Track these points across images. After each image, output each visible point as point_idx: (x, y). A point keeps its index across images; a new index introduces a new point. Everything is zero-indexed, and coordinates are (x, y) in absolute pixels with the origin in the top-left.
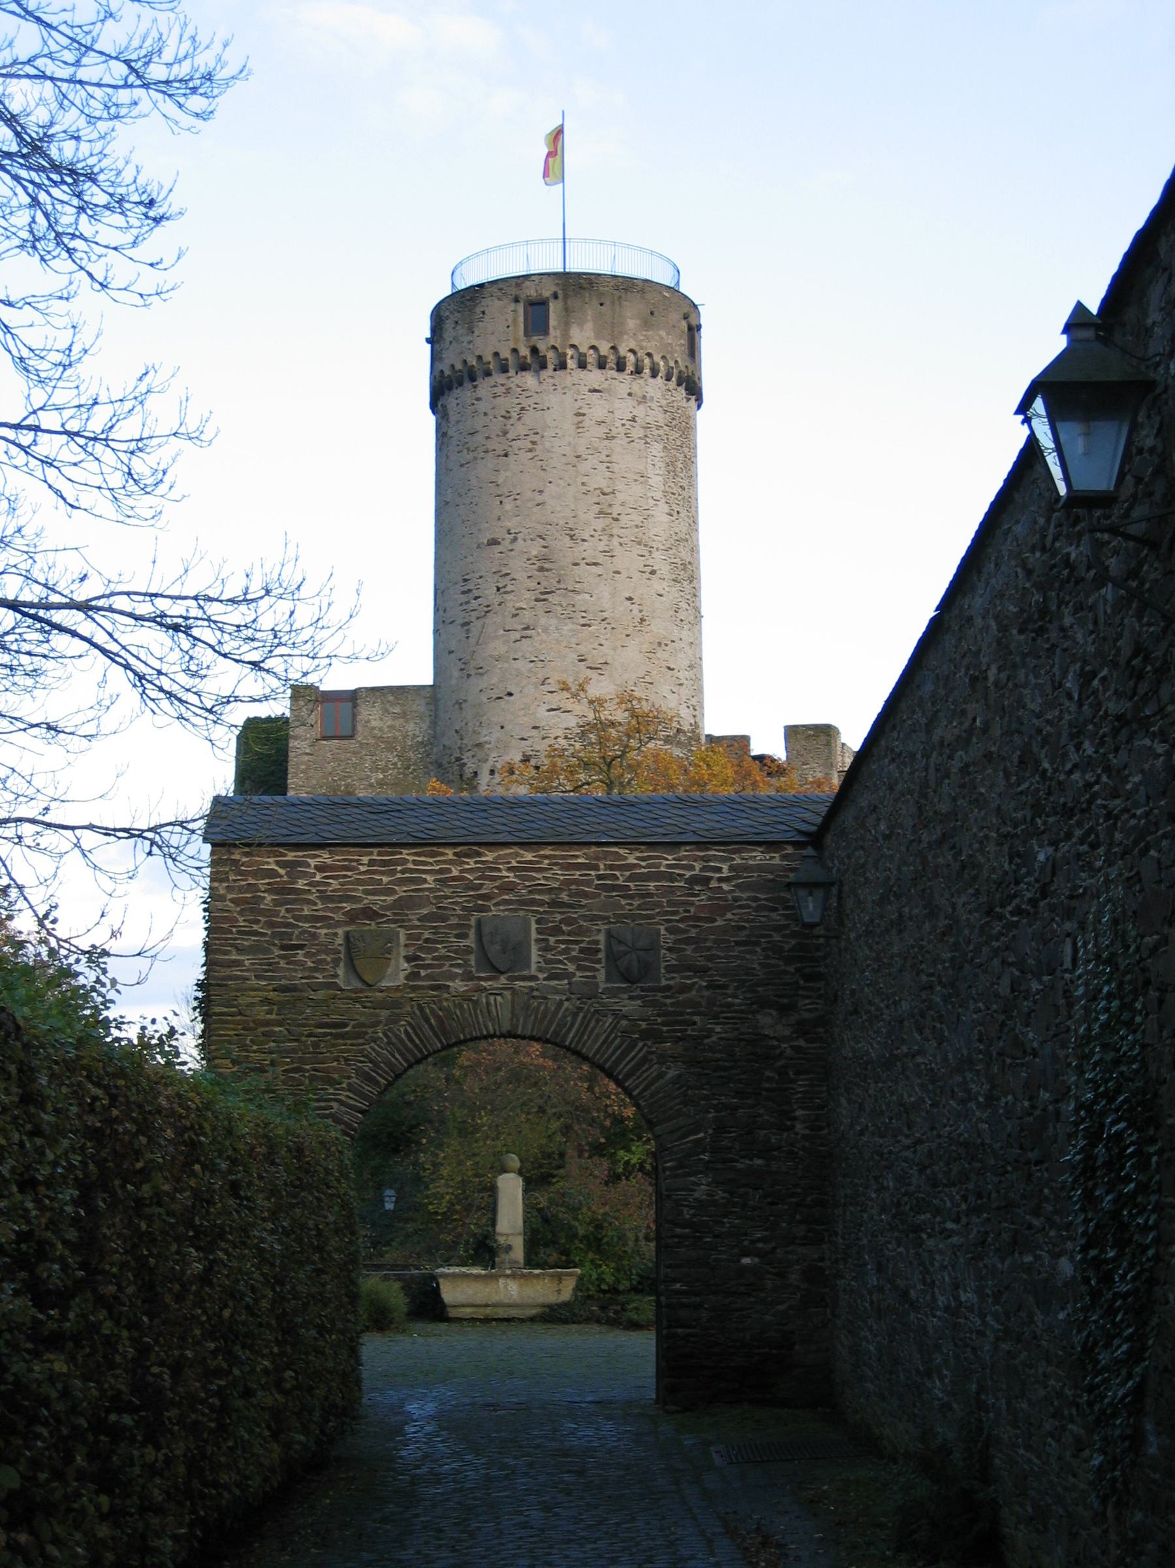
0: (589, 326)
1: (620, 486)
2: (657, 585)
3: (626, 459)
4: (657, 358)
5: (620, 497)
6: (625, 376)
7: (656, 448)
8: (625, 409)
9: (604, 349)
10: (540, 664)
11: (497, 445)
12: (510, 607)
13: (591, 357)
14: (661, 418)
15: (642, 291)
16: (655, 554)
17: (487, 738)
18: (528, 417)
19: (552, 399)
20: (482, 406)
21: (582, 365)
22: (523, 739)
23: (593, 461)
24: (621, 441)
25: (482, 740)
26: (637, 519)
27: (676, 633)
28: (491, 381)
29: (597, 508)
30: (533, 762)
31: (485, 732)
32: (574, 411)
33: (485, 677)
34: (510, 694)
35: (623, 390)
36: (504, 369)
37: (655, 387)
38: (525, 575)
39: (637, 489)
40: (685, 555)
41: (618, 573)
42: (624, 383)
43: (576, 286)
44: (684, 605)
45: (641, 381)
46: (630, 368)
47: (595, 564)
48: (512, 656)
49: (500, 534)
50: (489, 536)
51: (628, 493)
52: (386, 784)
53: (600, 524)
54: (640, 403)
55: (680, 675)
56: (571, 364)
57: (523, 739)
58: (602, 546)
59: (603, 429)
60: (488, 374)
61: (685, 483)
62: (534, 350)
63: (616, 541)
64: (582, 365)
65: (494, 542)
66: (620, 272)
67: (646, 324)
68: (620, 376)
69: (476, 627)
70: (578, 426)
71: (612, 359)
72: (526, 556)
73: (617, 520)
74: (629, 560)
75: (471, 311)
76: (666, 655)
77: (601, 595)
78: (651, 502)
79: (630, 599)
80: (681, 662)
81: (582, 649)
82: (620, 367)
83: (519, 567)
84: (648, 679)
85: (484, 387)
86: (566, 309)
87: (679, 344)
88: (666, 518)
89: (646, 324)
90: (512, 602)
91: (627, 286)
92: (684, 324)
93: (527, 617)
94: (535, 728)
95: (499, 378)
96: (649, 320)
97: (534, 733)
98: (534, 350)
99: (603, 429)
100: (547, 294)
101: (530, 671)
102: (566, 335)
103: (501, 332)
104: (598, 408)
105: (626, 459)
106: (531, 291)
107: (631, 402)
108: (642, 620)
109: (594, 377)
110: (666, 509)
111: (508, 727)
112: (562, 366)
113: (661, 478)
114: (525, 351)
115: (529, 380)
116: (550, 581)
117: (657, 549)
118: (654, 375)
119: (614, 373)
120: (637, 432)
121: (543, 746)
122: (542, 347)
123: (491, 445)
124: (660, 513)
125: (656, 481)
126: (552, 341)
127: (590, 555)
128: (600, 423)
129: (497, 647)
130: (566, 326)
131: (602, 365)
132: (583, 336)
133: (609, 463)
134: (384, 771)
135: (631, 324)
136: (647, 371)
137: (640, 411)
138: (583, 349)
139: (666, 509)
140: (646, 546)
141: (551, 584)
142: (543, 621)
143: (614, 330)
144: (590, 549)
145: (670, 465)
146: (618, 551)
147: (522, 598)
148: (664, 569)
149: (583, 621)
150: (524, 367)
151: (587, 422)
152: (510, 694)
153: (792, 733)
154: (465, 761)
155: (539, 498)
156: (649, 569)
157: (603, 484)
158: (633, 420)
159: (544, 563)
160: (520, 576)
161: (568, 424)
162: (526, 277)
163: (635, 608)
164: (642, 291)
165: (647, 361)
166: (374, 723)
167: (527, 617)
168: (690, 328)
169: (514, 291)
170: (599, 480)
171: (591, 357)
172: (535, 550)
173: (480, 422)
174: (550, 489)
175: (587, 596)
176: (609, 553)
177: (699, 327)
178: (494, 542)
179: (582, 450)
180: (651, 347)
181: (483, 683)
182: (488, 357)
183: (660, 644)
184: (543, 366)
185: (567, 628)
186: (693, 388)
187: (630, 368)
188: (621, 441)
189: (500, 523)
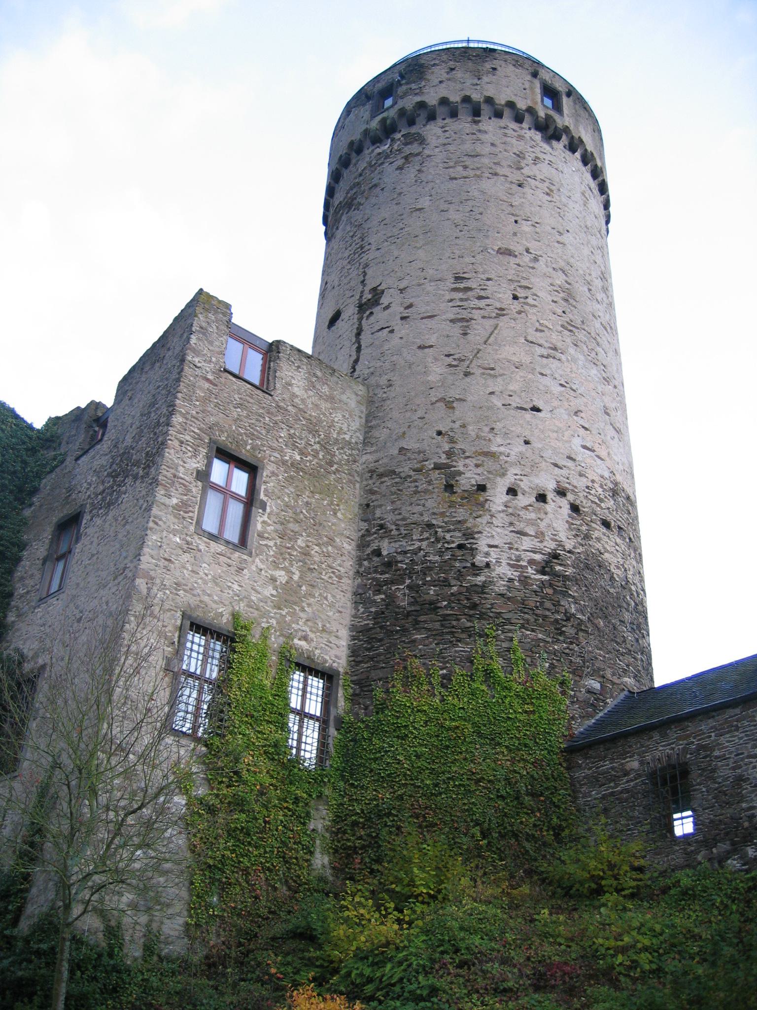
10: (572, 393)
17: (502, 449)
22: (556, 465)
25: (494, 449)
30: (570, 497)
31: (499, 440)
33: (499, 379)
34: (536, 409)
38: (550, 298)
48: (538, 369)
50: (499, 244)
52: (302, 470)
57: (556, 465)
65: (509, 253)
72: (550, 281)
94: (569, 458)
97: (570, 464)
101: (561, 392)
111: (536, 444)
121: (581, 483)
134: (301, 453)
142: (572, 350)
152: (536, 409)
154: (461, 469)
166: (296, 390)
172: (560, 279)
181: (497, 385)
189: (515, 239)
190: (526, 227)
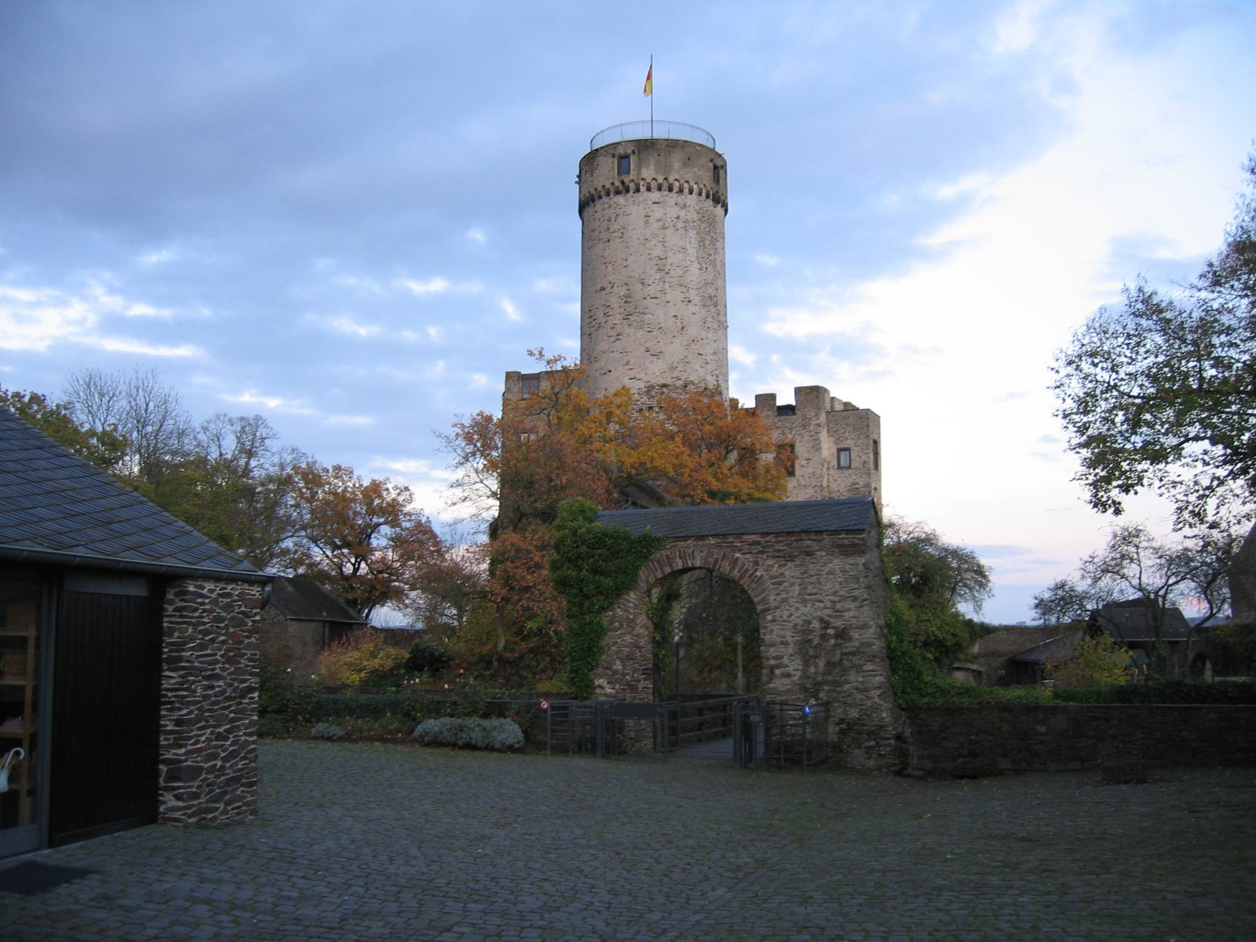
0: (652, 168)
1: (670, 254)
2: (692, 308)
3: (673, 240)
4: (692, 183)
5: (670, 261)
6: (673, 194)
7: (692, 233)
8: (673, 212)
9: (660, 179)
11: (604, 236)
12: (610, 324)
13: (654, 185)
14: (695, 217)
15: (683, 147)
18: (619, 219)
19: (633, 209)
20: (598, 216)
21: (649, 189)
23: (654, 242)
24: (670, 230)
27: (704, 335)
28: (601, 201)
32: (650, 217)
35: (672, 202)
36: (608, 194)
37: (692, 200)
39: (681, 256)
40: (711, 291)
42: (673, 198)
43: (645, 146)
44: (709, 319)
46: (676, 189)
49: (605, 284)
51: (674, 258)
53: (658, 276)
56: (643, 189)
58: (659, 288)
59: (661, 224)
60: (600, 198)
61: (712, 252)
62: (623, 183)
63: (667, 285)
64: (649, 189)
65: (603, 289)
66: (671, 137)
67: (685, 165)
68: (671, 194)
69: (594, 336)
70: (646, 222)
71: (665, 186)
74: (675, 295)
75: (592, 164)
77: (659, 315)
80: (708, 350)
81: (647, 345)
82: (671, 190)
83: (615, 302)
85: (599, 204)
86: (639, 159)
87: (707, 177)
88: (698, 272)
89: (685, 165)
90: (611, 321)
91: (673, 144)
92: (711, 165)
93: (619, 328)
95: (605, 199)
96: (687, 162)
98: (623, 183)
99: (661, 224)
100: (629, 151)
102: (639, 173)
103: (606, 173)
104: (657, 212)
105: (673, 240)
106: (621, 151)
107: (676, 208)
109: (655, 195)
112: (638, 190)
114: (617, 184)
115: (621, 199)
116: (630, 309)
118: (691, 192)
120: (680, 225)
122: (626, 181)
123: (602, 236)
125: (692, 251)
126: (631, 177)
127: (652, 293)
128: (658, 221)
129: (604, 346)
130: (639, 168)
131: (660, 189)
132: (648, 173)
133: (663, 242)
135: (676, 165)
136: (686, 191)
137: (682, 213)
138: (649, 180)
141: (632, 309)
143: (666, 169)
144: (652, 290)
145: (702, 243)
146: (668, 290)
147: (616, 319)
148: (696, 300)
150: (618, 192)
151: (651, 220)
153: (799, 391)
155: (625, 263)
157: (660, 254)
159: (627, 299)
160: (616, 306)
161: (641, 223)
162: (618, 143)
163: (679, 322)
164: (683, 147)
165: (686, 185)
167: (619, 328)
168: (715, 167)
169: (612, 151)
170: (658, 252)
171: (654, 185)
173: (597, 223)
174: (631, 259)
176: (663, 292)
177: (724, 166)
178: (603, 289)
179: (648, 236)
180: (688, 177)
182: (600, 189)
184: (628, 191)
185: (640, 333)
186: (719, 200)
187: (676, 189)
188: (670, 230)
190: (610, 268)
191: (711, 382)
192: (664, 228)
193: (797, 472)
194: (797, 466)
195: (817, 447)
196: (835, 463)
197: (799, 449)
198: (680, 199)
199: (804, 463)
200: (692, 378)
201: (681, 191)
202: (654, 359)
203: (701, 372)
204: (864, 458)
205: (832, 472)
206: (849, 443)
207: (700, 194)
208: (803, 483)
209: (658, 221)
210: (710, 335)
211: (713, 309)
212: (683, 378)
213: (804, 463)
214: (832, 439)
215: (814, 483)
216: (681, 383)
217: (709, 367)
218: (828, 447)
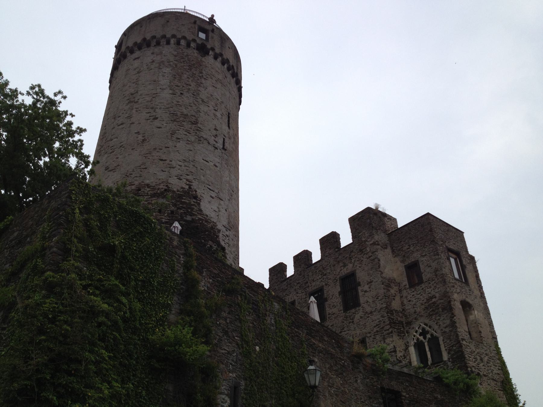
2: (157, 123)
5: (140, 93)
14: (172, 59)
16: (157, 110)
26: (148, 99)
29: (127, 102)
41: (133, 123)
45: (161, 47)
46: (154, 43)
47: (122, 124)
54: (157, 55)
55: (173, 163)
59: (137, 70)
63: (134, 111)
64: (132, 52)
73: (137, 102)
76: (158, 154)
78: (159, 90)
79: (139, 132)
82: (148, 45)
84: (142, 167)
104: (136, 64)
108: (143, 140)
109: (137, 54)
110: (171, 92)
113: (168, 81)
117: (160, 108)
119: (146, 49)
124: (166, 94)
125: (164, 82)
128: (135, 69)
137: (158, 58)
139: (171, 92)
140: (152, 108)
149: (111, 151)
156: (152, 118)
157: (132, 91)
158: (153, 62)
175: (116, 139)
183: (155, 149)
191: (176, 184)
192: (138, 73)
193: (362, 300)
194: (361, 294)
195: (376, 266)
196: (406, 282)
197: (362, 276)
198: (156, 50)
199: (366, 287)
200: (147, 182)
201: (158, 44)
202: (112, 172)
203: (163, 176)
204: (434, 265)
205: (404, 293)
206: (416, 256)
207: (178, 43)
208: (368, 309)
209: (135, 69)
210: (178, 145)
211: (187, 126)
212: (136, 183)
213: (366, 287)
214: (397, 259)
215: (379, 307)
216: (133, 187)
217: (174, 172)
218: (392, 268)
